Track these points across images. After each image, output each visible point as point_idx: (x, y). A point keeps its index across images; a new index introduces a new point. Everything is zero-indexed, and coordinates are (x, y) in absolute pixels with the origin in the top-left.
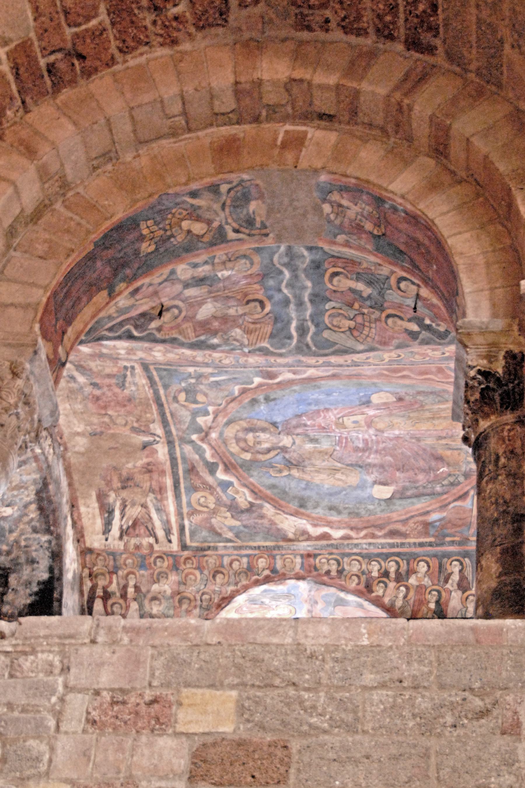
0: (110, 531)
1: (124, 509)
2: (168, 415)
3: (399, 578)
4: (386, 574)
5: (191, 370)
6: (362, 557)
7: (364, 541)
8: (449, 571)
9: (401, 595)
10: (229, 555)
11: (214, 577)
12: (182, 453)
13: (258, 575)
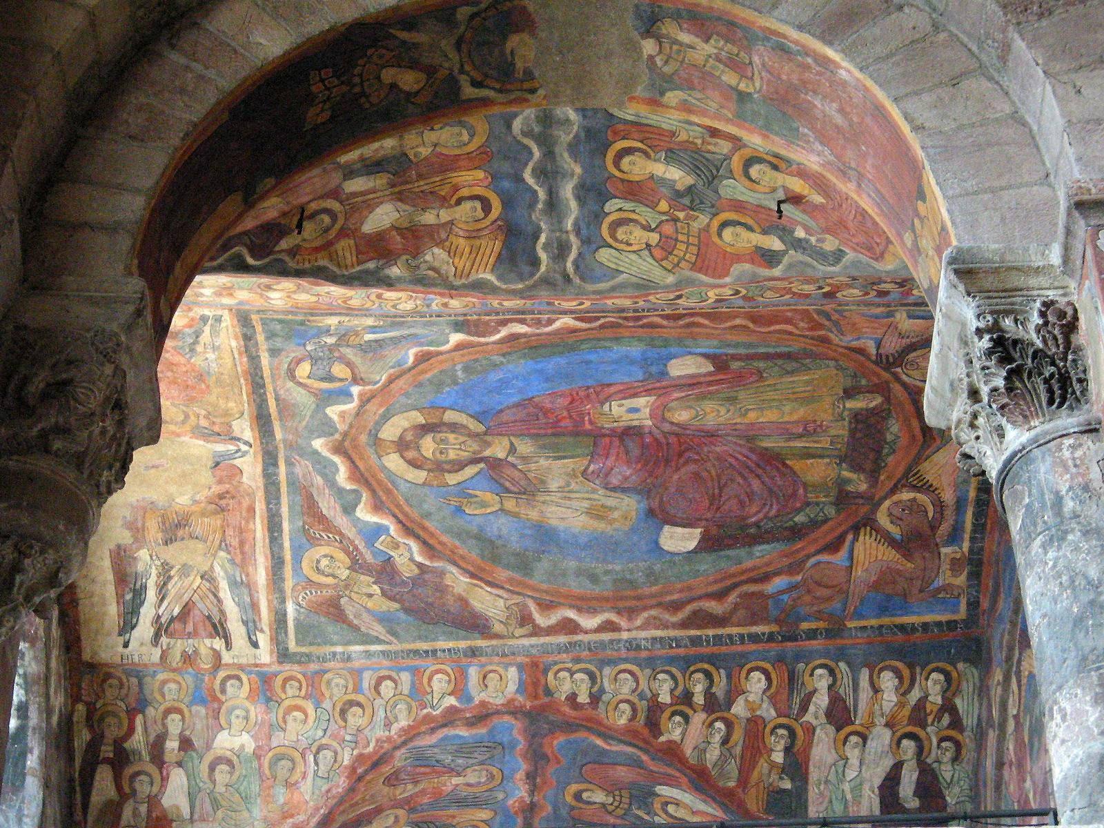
0: (133, 628)
1: (165, 584)
2: (272, 404)
3: (713, 705)
4: (687, 697)
5: (332, 321)
6: (639, 665)
7: (643, 634)
8: (810, 689)
9: (717, 738)
11: (343, 713)
13: (432, 707)
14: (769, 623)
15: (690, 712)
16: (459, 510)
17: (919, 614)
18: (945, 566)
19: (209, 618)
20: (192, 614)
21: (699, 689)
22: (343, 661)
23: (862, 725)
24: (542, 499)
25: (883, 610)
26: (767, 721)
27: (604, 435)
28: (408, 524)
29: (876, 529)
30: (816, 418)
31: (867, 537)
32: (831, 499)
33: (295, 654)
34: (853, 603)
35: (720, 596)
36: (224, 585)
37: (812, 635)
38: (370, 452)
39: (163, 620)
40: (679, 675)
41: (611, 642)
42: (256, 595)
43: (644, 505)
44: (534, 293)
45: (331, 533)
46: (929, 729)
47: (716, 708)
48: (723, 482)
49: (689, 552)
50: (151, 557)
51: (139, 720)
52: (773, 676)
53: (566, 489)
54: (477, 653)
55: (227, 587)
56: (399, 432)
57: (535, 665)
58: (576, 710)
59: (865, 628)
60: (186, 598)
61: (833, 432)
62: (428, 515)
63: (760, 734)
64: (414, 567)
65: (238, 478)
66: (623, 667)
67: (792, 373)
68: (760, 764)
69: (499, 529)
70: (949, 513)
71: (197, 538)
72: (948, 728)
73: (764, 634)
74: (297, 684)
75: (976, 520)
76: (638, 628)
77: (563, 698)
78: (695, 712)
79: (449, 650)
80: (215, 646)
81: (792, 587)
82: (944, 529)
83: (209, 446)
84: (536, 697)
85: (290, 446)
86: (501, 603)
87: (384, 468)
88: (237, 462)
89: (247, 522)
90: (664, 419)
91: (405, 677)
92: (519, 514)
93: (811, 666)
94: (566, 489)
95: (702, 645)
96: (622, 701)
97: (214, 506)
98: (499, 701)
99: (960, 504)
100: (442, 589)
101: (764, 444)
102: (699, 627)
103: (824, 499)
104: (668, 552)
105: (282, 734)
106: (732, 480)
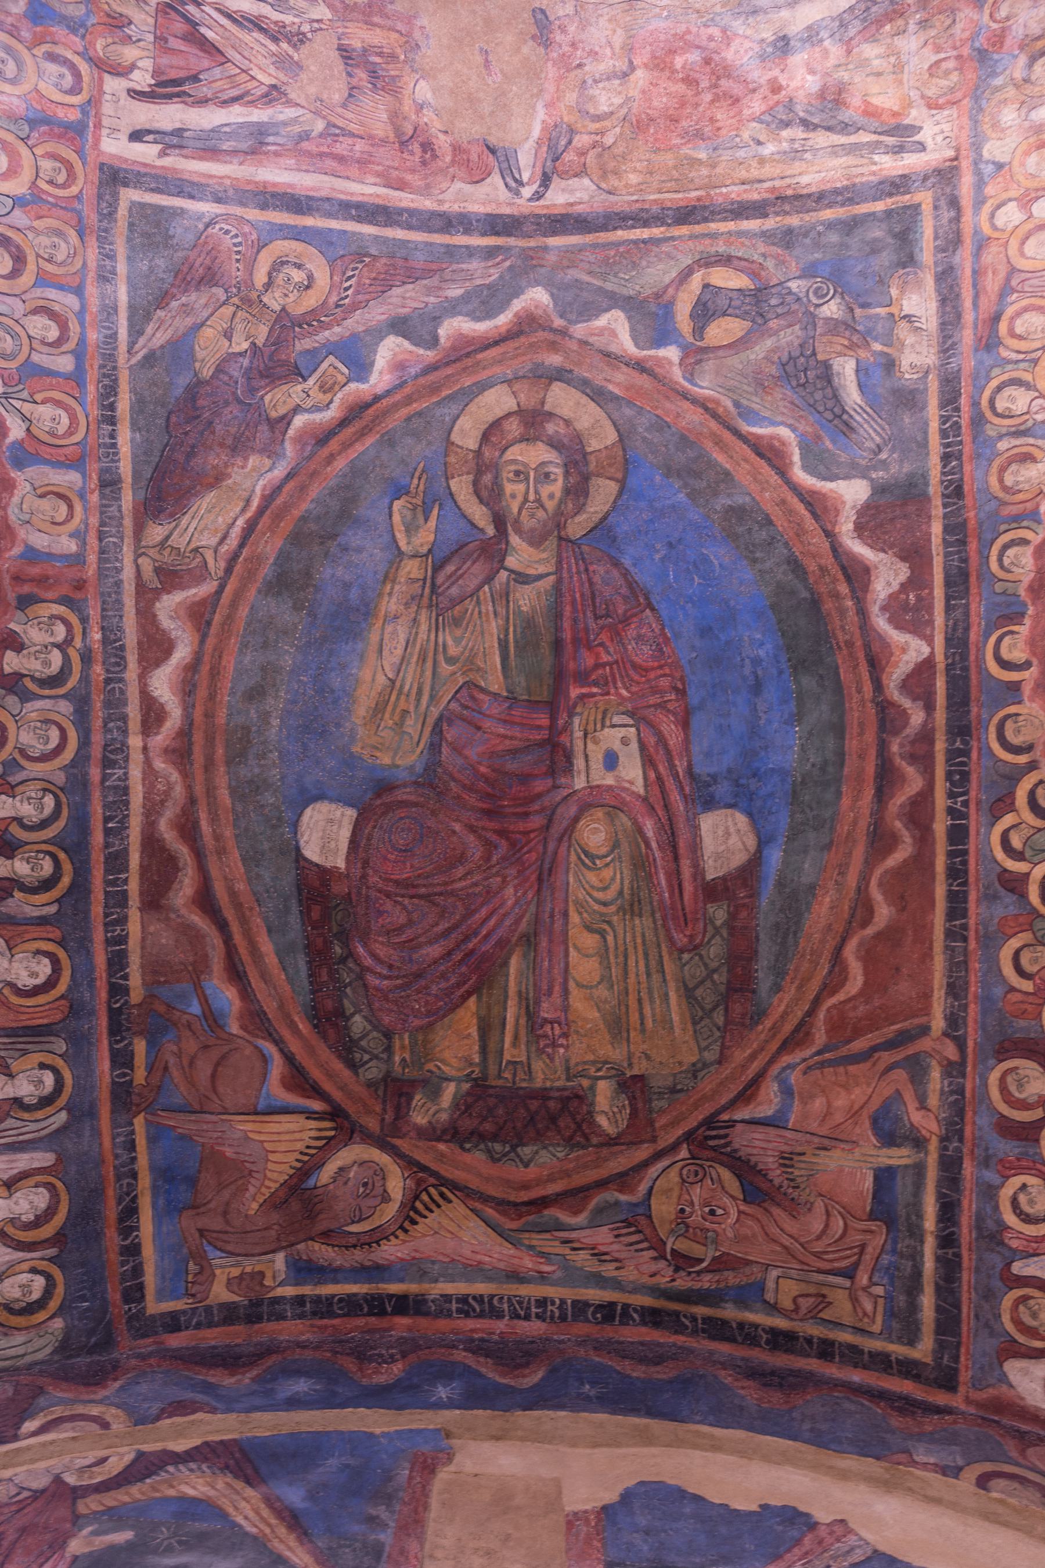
1: (261, 30)
6: (73, 763)
7: (136, 773)
8: (15, 1066)
10: (81, 314)
12: (471, 252)
14: (145, 983)
16: (400, 491)
17: (157, 1234)
18: (250, 1266)
19: (195, 78)
21: (21, 867)
22: (101, 267)
24: (423, 617)
27: (553, 718)
28: (371, 411)
29: (328, 1146)
30: (573, 1038)
31: (313, 1134)
32: (397, 1069)
33: (115, 196)
34: (185, 1124)
35: (205, 900)
36: (259, 115)
37: (122, 1059)
38: (523, 365)
40: (50, 833)
41: (124, 718)
42: (235, 160)
43: (403, 775)
45: (357, 292)
49: (298, 849)
50: (318, 21)
52: (41, 999)
53: (441, 658)
54: (107, 491)
55: (254, 118)
56: (566, 412)
57: (80, 585)
59: (131, 1146)
60: (231, 53)
61: (538, 1066)
62: (389, 441)
64: (282, 411)
65: (462, 173)
66: (72, 735)
67: (688, 993)
69: (359, 550)
70: (359, 1256)
71: (350, 95)
73: (126, 977)
75: (341, 1300)
76: (148, 762)
79: (114, 445)
80: (136, 72)
81: (212, 1018)
82: (323, 1253)
83: (530, 144)
86: (208, 540)
87: (483, 387)
88: (496, 179)
89: (378, 175)
90: (585, 808)
91: (65, 363)
92: (394, 581)
93: (60, 1063)
94: (441, 658)
95: (107, 871)
97: (410, 133)
99: (376, 1271)
100: (239, 446)
102: (144, 869)
103: (397, 1059)
104: (300, 815)
106: (442, 915)
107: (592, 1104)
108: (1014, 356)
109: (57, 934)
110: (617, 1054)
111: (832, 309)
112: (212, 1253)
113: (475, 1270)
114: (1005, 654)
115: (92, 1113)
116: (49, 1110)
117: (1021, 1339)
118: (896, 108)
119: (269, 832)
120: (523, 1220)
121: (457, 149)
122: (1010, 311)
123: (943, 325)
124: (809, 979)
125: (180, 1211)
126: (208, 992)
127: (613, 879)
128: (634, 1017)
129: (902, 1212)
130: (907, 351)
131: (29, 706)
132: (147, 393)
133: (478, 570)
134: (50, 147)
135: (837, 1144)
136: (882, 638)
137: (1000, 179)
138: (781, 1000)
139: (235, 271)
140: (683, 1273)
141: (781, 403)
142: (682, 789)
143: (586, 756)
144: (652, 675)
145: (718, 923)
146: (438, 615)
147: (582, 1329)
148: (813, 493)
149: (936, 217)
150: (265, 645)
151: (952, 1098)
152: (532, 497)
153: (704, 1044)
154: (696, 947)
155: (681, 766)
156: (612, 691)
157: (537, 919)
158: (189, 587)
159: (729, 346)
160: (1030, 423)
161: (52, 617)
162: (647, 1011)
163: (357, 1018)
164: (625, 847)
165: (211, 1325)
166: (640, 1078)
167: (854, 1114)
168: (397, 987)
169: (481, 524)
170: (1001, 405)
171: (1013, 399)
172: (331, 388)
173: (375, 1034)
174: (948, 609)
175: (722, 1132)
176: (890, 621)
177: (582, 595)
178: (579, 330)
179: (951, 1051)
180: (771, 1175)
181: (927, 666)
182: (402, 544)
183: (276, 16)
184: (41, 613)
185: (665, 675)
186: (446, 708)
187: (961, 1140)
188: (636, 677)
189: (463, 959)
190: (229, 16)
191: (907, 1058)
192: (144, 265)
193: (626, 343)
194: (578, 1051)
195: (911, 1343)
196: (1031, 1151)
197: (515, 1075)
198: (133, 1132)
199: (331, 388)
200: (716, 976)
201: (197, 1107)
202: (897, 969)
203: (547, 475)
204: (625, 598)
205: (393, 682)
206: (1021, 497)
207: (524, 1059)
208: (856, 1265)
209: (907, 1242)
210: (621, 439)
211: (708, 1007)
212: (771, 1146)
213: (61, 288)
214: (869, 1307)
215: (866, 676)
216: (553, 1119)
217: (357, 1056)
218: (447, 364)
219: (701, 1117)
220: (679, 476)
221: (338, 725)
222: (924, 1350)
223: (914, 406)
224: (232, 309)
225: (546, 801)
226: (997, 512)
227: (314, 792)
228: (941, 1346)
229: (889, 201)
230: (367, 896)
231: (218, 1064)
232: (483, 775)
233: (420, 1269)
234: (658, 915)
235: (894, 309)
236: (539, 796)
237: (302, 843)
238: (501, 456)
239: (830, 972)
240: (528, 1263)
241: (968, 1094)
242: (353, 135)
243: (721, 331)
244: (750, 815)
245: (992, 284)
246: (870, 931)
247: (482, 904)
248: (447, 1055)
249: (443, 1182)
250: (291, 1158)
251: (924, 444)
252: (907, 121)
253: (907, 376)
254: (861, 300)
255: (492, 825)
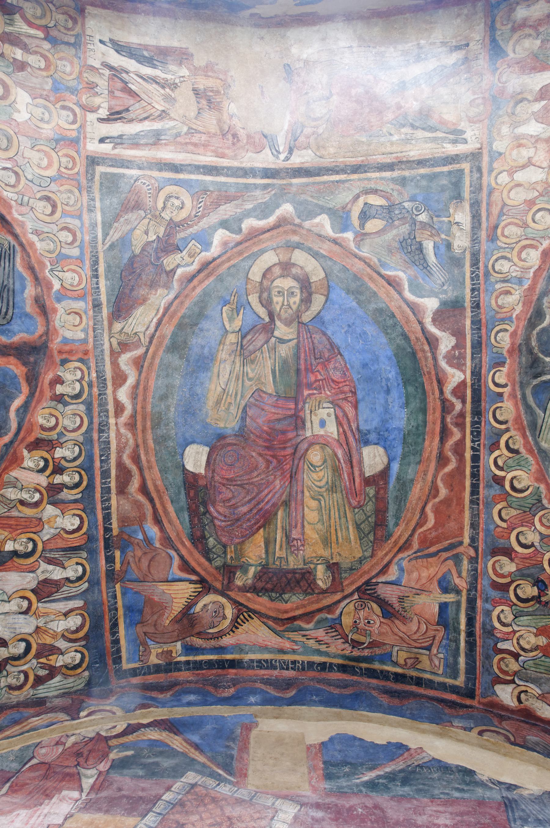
0: (117, 51)
1: (157, 83)
4: (59, 470)
8: (66, 564)
11: (47, 199)
12: (256, 186)
13: (52, 270)
15: (48, 472)
16: (226, 303)
17: (126, 635)
18: (166, 648)
19: (127, 110)
20: (130, 98)
21: (65, 478)
22: (89, 205)
23: (37, 608)
24: (237, 360)
25: (129, 609)
26: (40, 534)
27: (296, 404)
28: (212, 265)
29: (199, 595)
31: (193, 590)
32: (229, 561)
33: (94, 170)
34: (136, 586)
35: (144, 489)
36: (157, 126)
37: (110, 560)
38: (281, 241)
39: (124, 75)
40: (77, 463)
41: (107, 411)
42: (147, 149)
43: (229, 432)
44: (524, 353)
45: (204, 209)
46: (34, 661)
47: (51, 493)
48: (247, 486)
49: (184, 466)
50: (183, 77)
51: (40, 34)
52: (76, 535)
53: (245, 378)
54: (96, 309)
56: (301, 263)
57: (86, 353)
58: (50, 384)
59: (115, 597)
60: (143, 96)
61: (291, 559)
62: (220, 279)
63: (29, 530)
64: (172, 267)
66: (86, 420)
67: (358, 526)
68: (3, 532)
69: (208, 330)
70: (213, 643)
71: (199, 113)
72: (36, 676)
73: (111, 524)
74: (70, 166)
75: (205, 662)
76: (118, 430)
77: (59, 373)
78: (48, 477)
79: (98, 288)
81: (148, 541)
82: (198, 642)
83: (283, 133)
84: (60, 352)
85: (283, 188)
87: (263, 252)
88: (267, 151)
89: (213, 151)
90: (311, 444)
91: (75, 252)
92: (224, 344)
93: (84, 562)
94: (245, 378)
95: (102, 478)
96: (57, 419)
97: (227, 130)
98: (57, 324)
99: (221, 650)
100: (153, 285)
101: (280, 514)
102: (117, 477)
103: (229, 557)
105: (29, 145)
106: (248, 493)
107: (315, 575)
108: (504, 245)
109: (81, 507)
110: (326, 553)
111: (423, 217)
112: (150, 642)
113: (265, 648)
114: (497, 380)
115: (98, 583)
116: (81, 582)
117: (501, 676)
118: (454, 121)
119: (171, 458)
120: (285, 626)
121: (249, 136)
122: (502, 224)
123: (473, 228)
124: (411, 520)
125: (136, 624)
126: (146, 529)
127: (324, 476)
128: (334, 537)
129: (451, 622)
130: (457, 239)
131: (67, 408)
132: (111, 263)
133: (262, 338)
134: (65, 151)
135: (423, 592)
136: (443, 371)
137: (500, 160)
138: (398, 530)
139: (148, 202)
140: (356, 649)
141: (399, 260)
142: (354, 436)
143: (311, 421)
144: (341, 385)
145: (371, 496)
146: (244, 359)
147: (311, 674)
148: (414, 303)
149: (471, 176)
150: (167, 376)
151: (472, 573)
152: (286, 303)
153: (364, 549)
154: (361, 506)
155: (354, 427)
156: (323, 392)
157: (290, 494)
158: (133, 351)
159: (376, 233)
160: (509, 277)
161: (75, 368)
162: (339, 534)
163: (211, 539)
164: (329, 462)
165: (150, 674)
166: (336, 564)
167: (430, 579)
168: (228, 525)
169: (263, 316)
170: (497, 268)
171: (502, 266)
172: (194, 255)
173: (219, 546)
174: (473, 358)
175: (373, 587)
176: (447, 363)
177: (309, 349)
178: (307, 224)
179: (472, 553)
180: (395, 606)
181: (463, 383)
182: (227, 327)
183: (163, 76)
184: (71, 367)
185: (346, 385)
186: (248, 401)
187: (476, 591)
188: (334, 386)
189: (257, 512)
190: (141, 77)
191: (453, 555)
192: (108, 202)
193: (328, 230)
194: (308, 552)
195: (455, 678)
196: (505, 596)
197: (281, 563)
198: (115, 591)
199: (194, 255)
200: (370, 519)
201: (142, 579)
202: (449, 517)
203: (293, 293)
204: (329, 350)
205: (224, 390)
206: (504, 310)
207: (285, 556)
208: (431, 645)
209: (453, 634)
210: (326, 276)
211: (366, 532)
212: (394, 593)
213: (72, 217)
214: (437, 663)
215: (436, 388)
216: (298, 582)
217: (211, 556)
218: (246, 241)
219: (363, 581)
220: (353, 294)
221: (200, 410)
222: (460, 681)
223: (459, 265)
224: (148, 220)
225: (294, 442)
226: (493, 317)
227: (190, 440)
228: (468, 679)
229: (450, 167)
230: (215, 486)
231: (150, 561)
232: (265, 431)
233: (240, 648)
234: (344, 492)
235: (451, 219)
236: (290, 439)
237: (185, 463)
238: (271, 284)
239: (420, 518)
240: (287, 645)
241: (479, 571)
242: (200, 132)
243: (373, 225)
244: (385, 448)
245: (495, 211)
246: (437, 500)
247: (266, 488)
248: (251, 555)
249: (250, 610)
250: (183, 601)
251: (463, 283)
252: (459, 128)
253: (456, 251)
254: (437, 214)
255: (270, 453)
